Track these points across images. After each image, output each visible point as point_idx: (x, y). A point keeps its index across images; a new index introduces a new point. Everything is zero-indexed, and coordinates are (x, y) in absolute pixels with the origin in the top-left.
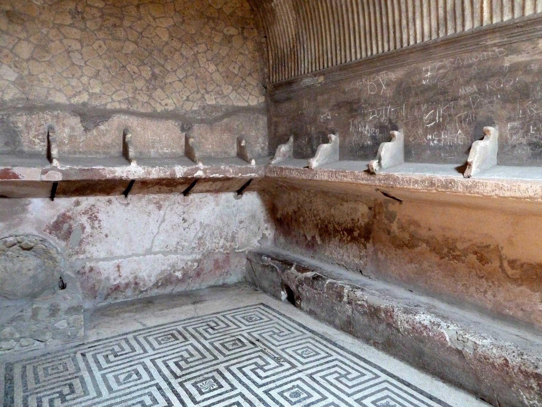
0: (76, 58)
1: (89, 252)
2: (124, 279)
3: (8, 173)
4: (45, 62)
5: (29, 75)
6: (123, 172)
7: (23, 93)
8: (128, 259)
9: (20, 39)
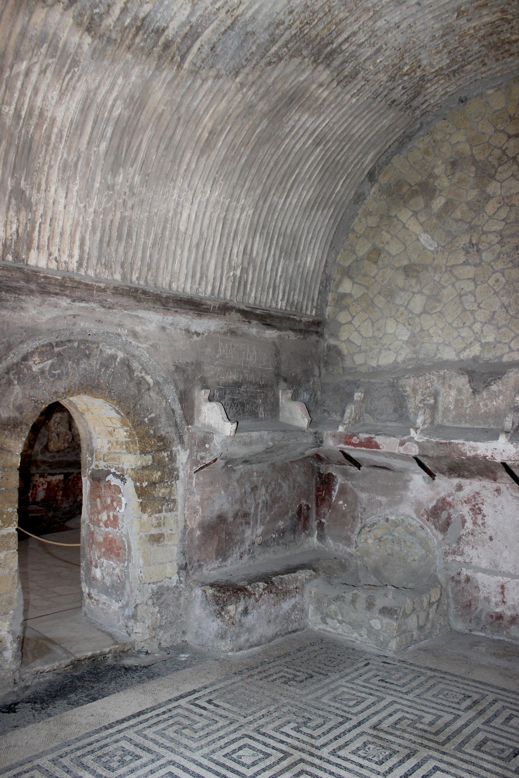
0: (469, 303)
1: (468, 555)
2: (509, 608)
4: (435, 313)
5: (421, 331)
7: (415, 352)
8: (516, 580)
9: (414, 293)
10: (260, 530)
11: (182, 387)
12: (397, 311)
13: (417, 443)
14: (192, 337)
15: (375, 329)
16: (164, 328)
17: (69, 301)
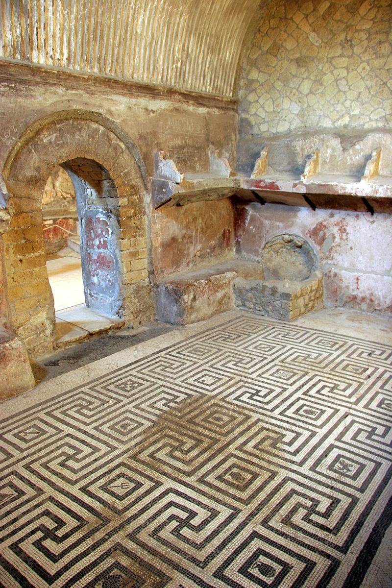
1: (336, 260)
2: (361, 292)
3: (273, 185)
6: (352, 189)
8: (367, 274)
9: (303, 79)
10: (199, 247)
11: (144, 150)
12: (291, 92)
13: (305, 185)
14: (149, 114)
15: (275, 105)
16: (130, 108)
17: (64, 89)
